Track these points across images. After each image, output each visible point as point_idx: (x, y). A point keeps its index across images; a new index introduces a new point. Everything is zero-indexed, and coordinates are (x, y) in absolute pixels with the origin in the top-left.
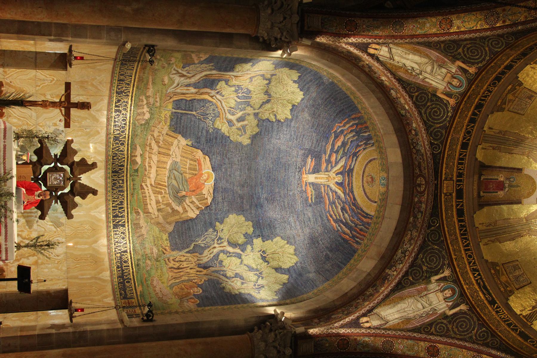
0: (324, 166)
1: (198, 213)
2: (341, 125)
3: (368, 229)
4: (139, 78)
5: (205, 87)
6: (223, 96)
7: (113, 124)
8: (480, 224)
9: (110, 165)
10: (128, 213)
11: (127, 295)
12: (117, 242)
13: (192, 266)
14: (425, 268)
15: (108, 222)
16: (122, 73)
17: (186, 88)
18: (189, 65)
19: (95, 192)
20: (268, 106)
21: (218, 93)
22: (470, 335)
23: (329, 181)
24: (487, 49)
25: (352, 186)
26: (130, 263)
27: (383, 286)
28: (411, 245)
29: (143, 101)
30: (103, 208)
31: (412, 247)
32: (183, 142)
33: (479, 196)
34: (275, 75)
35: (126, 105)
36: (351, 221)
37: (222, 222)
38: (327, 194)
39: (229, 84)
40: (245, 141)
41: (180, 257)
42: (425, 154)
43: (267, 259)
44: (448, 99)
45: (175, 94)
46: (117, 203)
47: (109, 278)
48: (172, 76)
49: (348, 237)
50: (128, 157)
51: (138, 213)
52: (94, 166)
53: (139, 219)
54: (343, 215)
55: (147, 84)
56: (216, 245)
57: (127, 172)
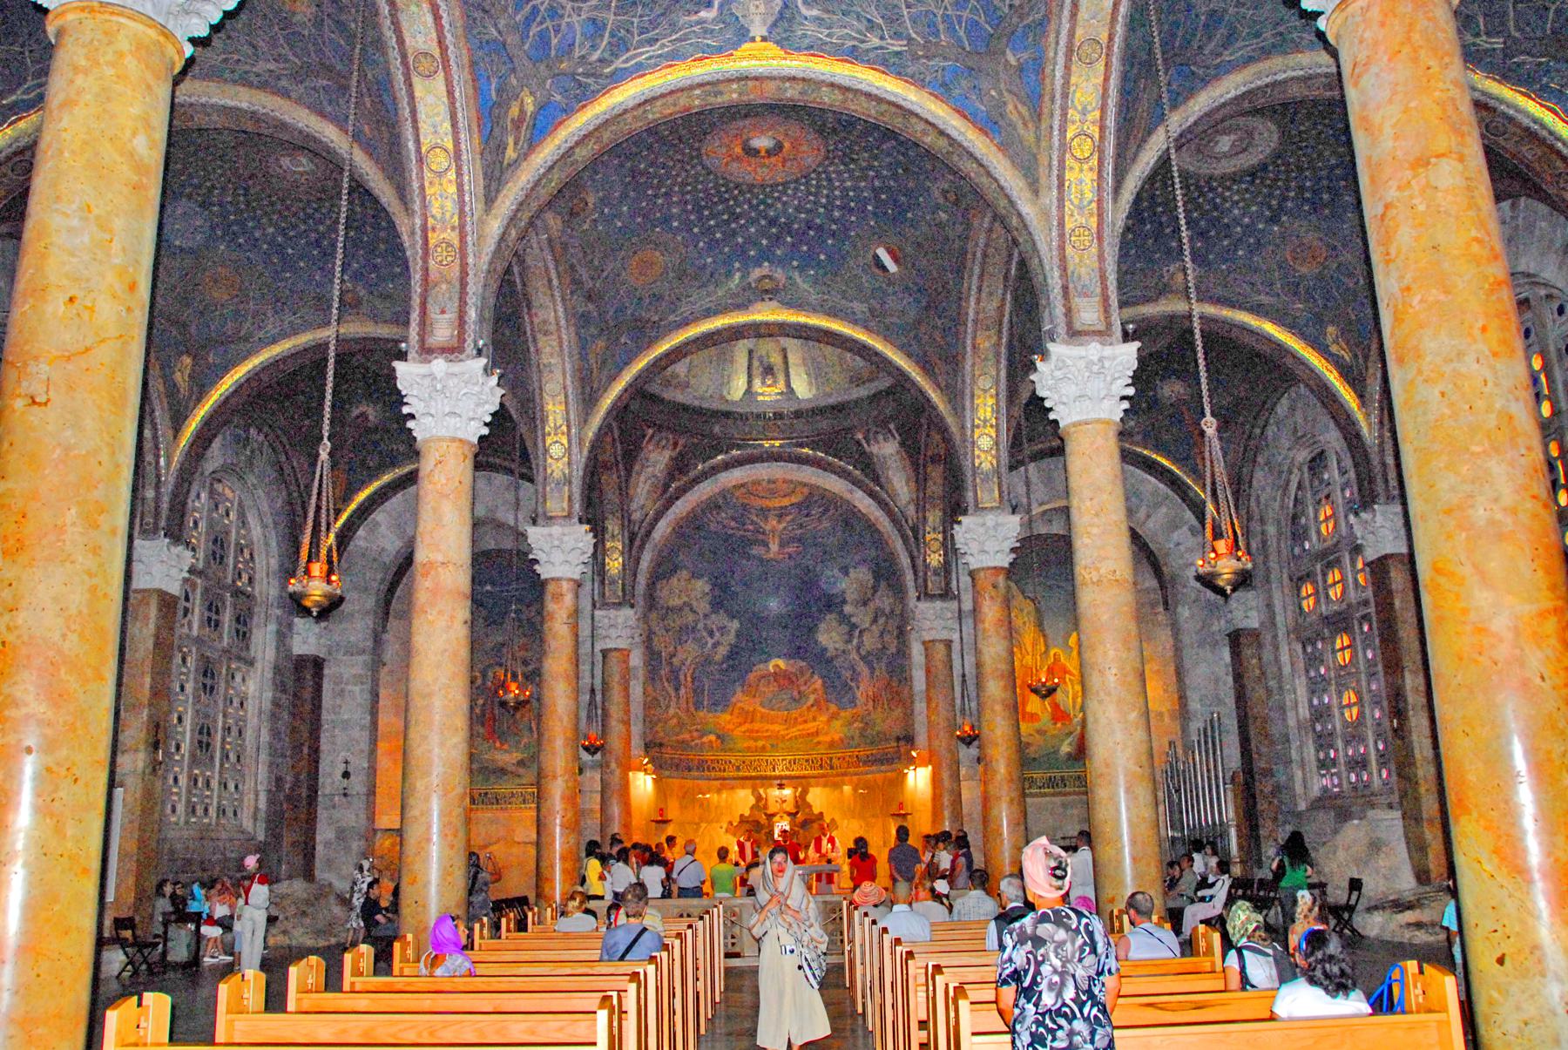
0: (761, 537)
20: (695, 604)
51: (819, 743)
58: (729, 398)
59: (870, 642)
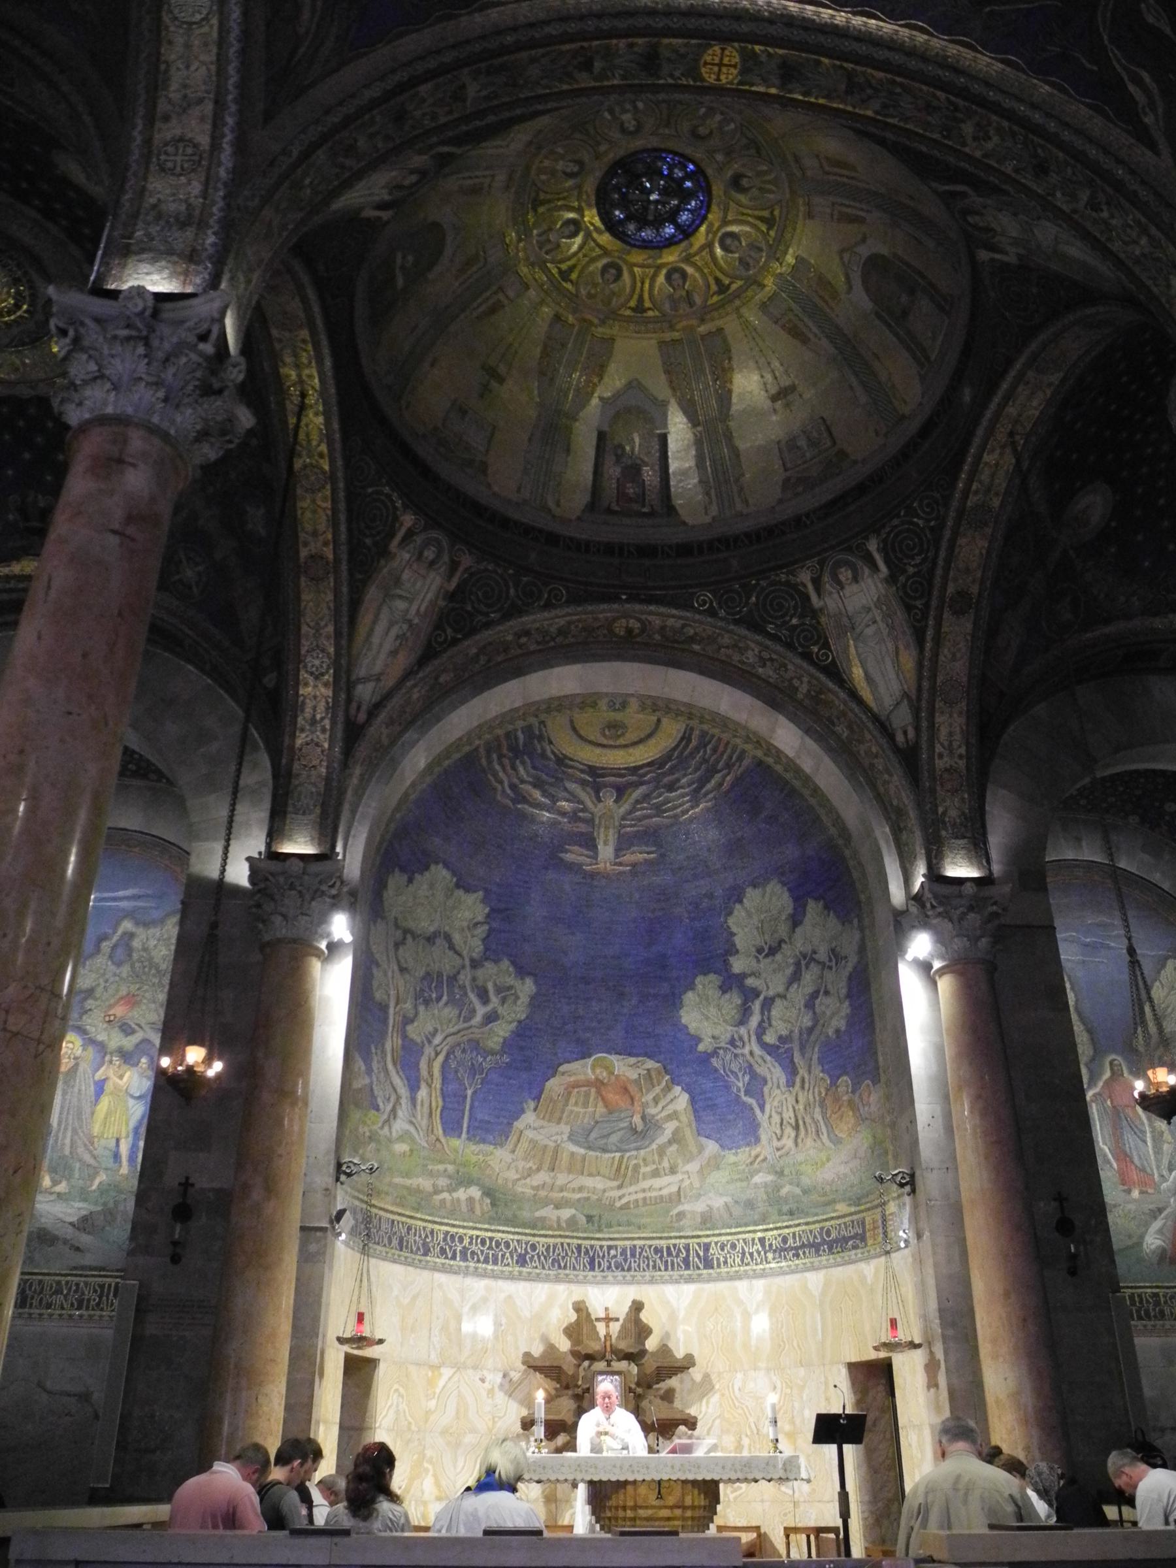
0: (583, 828)
1: (679, 1088)
2: (499, 787)
3: (713, 736)
4: (397, 1205)
5: (416, 1066)
6: (436, 1031)
7: (490, 1267)
8: (706, 513)
9: (577, 1276)
10: (680, 1237)
11: (857, 1234)
12: (742, 1261)
13: (791, 1100)
14: (794, 621)
15: (699, 1279)
16: (386, 1241)
17: (419, 1107)
18: (373, 1096)
19: (637, 1307)
20: (457, 938)
21: (430, 1042)
22: (928, 532)
23: (612, 817)
24: (370, 490)
25: (625, 769)
26: (787, 1231)
27: (832, 701)
28: (747, 648)
29: (443, 1201)
30: (670, 1290)
31: (752, 645)
32: (529, 1117)
33: (652, 514)
34: (396, 919)
35: (453, 1237)
36: (697, 769)
37: (698, 1040)
38: (640, 820)
39: (411, 1015)
40: (527, 988)
41: (773, 1122)
42: (568, 618)
43: (774, 945)
44: (461, 569)
45: (430, 1130)
46: (658, 1261)
47: (823, 1272)
48: (394, 1134)
49: (728, 778)
50: (561, 1236)
51: (681, 1215)
52: (580, 1308)
53: (693, 1212)
54: (682, 787)
55: (408, 1188)
56: (746, 1051)
57: (592, 1239)
58: (557, 512)
59: (779, 1027)
